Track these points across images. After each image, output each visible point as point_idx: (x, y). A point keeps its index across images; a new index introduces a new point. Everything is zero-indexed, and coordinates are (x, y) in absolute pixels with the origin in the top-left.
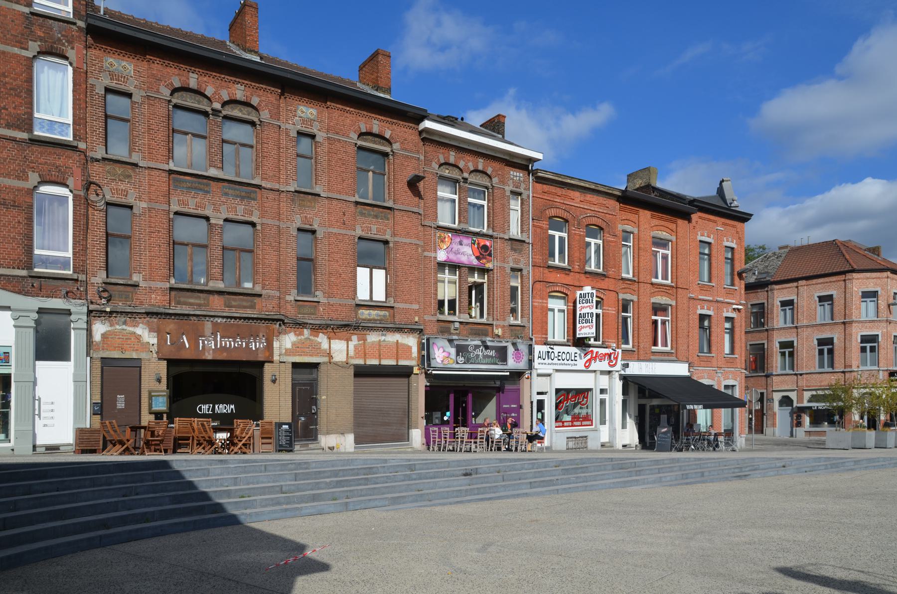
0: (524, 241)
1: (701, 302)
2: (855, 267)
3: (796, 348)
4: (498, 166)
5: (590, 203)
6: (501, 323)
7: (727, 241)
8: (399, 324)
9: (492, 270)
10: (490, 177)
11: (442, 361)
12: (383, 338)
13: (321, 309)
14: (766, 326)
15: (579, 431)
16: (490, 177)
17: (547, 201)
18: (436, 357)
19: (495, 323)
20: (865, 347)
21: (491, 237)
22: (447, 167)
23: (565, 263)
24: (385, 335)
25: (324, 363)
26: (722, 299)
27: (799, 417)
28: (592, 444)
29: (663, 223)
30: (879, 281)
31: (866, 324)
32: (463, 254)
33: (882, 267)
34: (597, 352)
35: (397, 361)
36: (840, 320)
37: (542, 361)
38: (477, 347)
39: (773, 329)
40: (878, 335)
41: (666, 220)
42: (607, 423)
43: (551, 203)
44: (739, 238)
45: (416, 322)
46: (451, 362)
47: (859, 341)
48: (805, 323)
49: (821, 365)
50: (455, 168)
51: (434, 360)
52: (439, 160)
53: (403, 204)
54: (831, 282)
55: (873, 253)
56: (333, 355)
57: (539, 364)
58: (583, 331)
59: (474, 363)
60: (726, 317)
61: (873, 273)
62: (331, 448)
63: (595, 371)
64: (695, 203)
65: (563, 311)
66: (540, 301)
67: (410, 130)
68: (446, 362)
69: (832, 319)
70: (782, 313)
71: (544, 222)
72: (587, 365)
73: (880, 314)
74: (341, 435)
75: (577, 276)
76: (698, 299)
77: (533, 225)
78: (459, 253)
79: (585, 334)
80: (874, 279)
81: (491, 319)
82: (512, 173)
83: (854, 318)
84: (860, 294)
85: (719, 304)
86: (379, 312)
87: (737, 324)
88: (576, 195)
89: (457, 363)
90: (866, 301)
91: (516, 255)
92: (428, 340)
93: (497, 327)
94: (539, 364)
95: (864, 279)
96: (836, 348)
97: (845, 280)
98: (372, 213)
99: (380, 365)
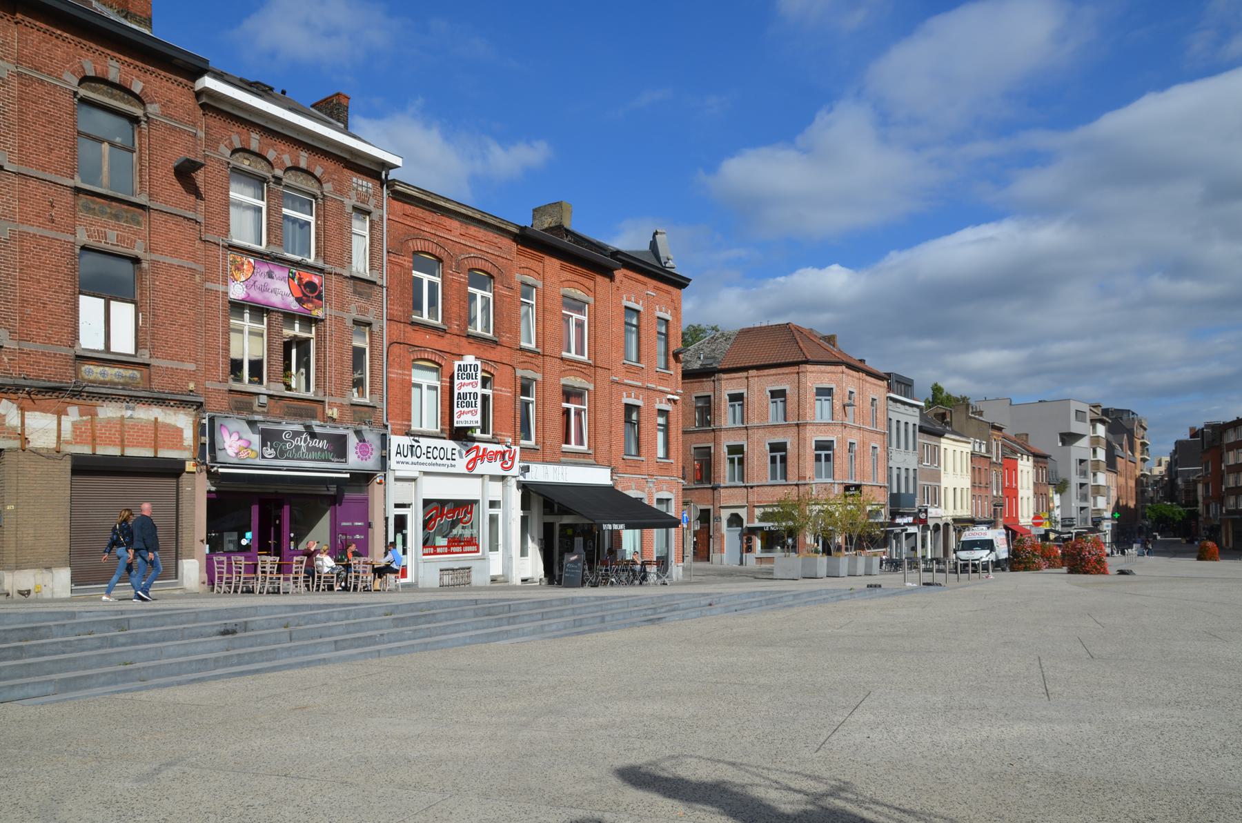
0: (374, 283)
1: (627, 388)
2: (809, 358)
3: (746, 453)
4: (333, 167)
5: (475, 238)
6: (338, 400)
7: (661, 311)
9: (322, 320)
10: (319, 180)
11: (237, 454)
13: (6, 360)
14: (712, 425)
15: (458, 560)
16: (319, 180)
17: (410, 228)
18: (226, 446)
19: (327, 400)
20: (820, 455)
21: (322, 270)
22: (247, 155)
23: (437, 320)
24: (133, 409)
25: (11, 450)
26: (654, 386)
27: (749, 540)
28: (477, 579)
29: (577, 278)
30: (834, 376)
32: (274, 291)
33: (837, 360)
34: (485, 450)
35: (156, 452)
37: (403, 459)
38: (296, 434)
39: (720, 430)
40: (833, 441)
41: (581, 275)
42: (500, 548)
43: (416, 232)
44: (675, 308)
45: (191, 391)
46: (253, 455)
47: (814, 447)
48: (756, 423)
49: (774, 477)
50: (260, 160)
51: (223, 451)
52: (232, 142)
53: (166, 202)
54: (783, 374)
55: (829, 342)
56: (30, 438)
57: (398, 462)
58: (464, 418)
59: (293, 459)
60: (659, 410)
62: (25, 593)
63: (482, 476)
64: (619, 256)
65: (436, 388)
66: (400, 372)
67: (180, 88)
68: (243, 455)
69: (785, 420)
70: (731, 409)
71: (405, 258)
72: (470, 466)
73: (835, 417)
74: (44, 571)
75: (456, 339)
76: (623, 384)
77: (389, 261)
78: (267, 290)
79: (466, 422)
81: (321, 394)
82: (355, 179)
84: (815, 391)
85: (651, 393)
86: (121, 370)
87: (673, 419)
88: (455, 224)
89: (263, 457)
90: (820, 400)
91: (362, 302)
93: (331, 405)
94: (398, 462)
95: (818, 372)
96: (789, 455)
97: (798, 373)
98: (109, 210)
99: (122, 456)
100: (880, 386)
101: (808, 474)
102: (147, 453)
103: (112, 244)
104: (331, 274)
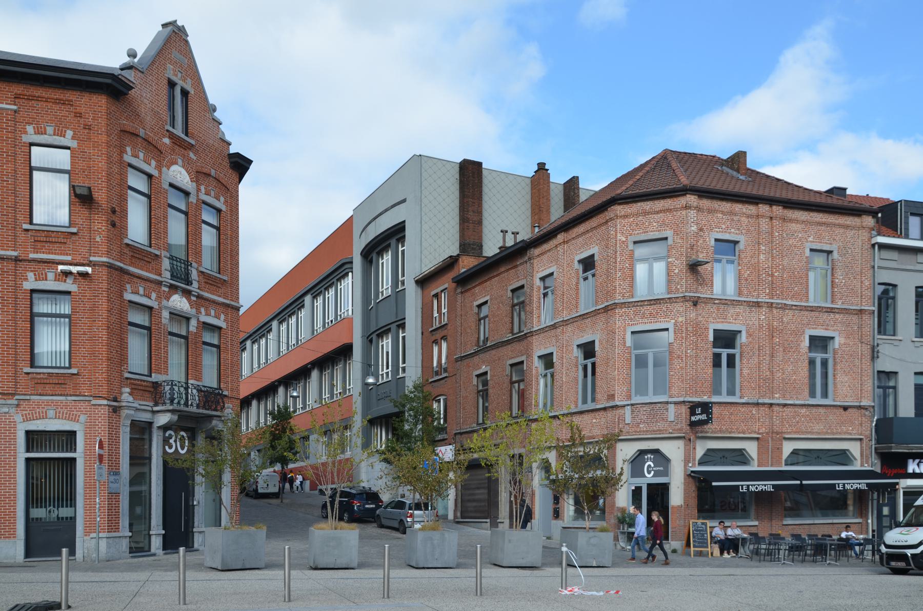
7: (38, 132)
31: (643, 309)
36: (603, 303)
39: (531, 334)
49: (585, 401)
61: (656, 202)
80: (658, 213)
83: (619, 299)
95: (637, 215)
100: (847, 227)
101: (619, 391)
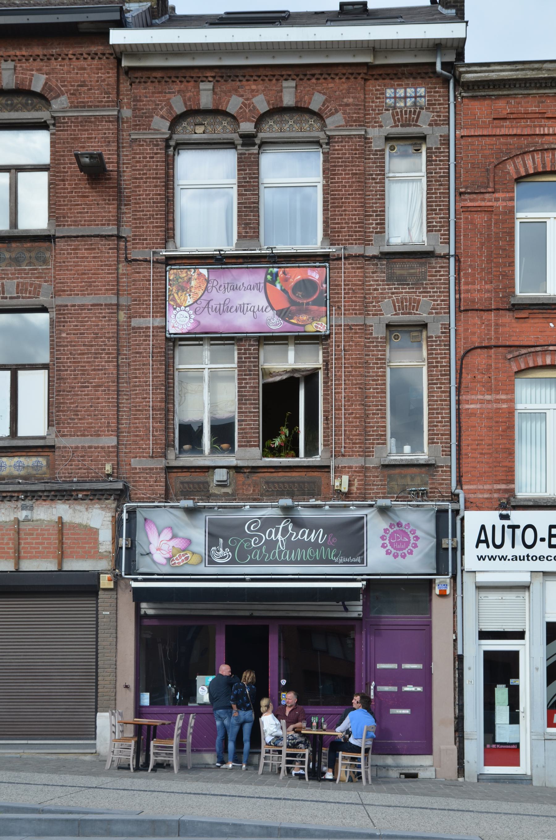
4: (345, 86)
6: (356, 462)
8: (65, 482)
11: (169, 559)
12: (22, 515)
16: (318, 115)
18: (153, 549)
19: (332, 464)
22: (199, 119)
24: (31, 508)
32: (241, 309)
35: (60, 564)
38: (268, 523)
45: (109, 475)
46: (194, 559)
50: (219, 118)
51: (147, 558)
52: (171, 107)
53: (76, 223)
59: (262, 562)
67: (95, 62)
68: (179, 561)
78: (229, 310)
86: (22, 459)
89: (212, 562)
92: (132, 513)
93: (339, 471)
98: (7, 255)
99: (17, 571)
102: (49, 565)
103: (11, 298)
104: (339, 259)
